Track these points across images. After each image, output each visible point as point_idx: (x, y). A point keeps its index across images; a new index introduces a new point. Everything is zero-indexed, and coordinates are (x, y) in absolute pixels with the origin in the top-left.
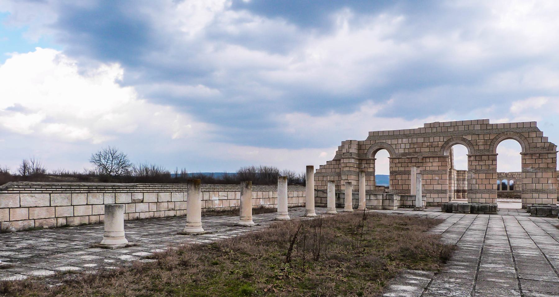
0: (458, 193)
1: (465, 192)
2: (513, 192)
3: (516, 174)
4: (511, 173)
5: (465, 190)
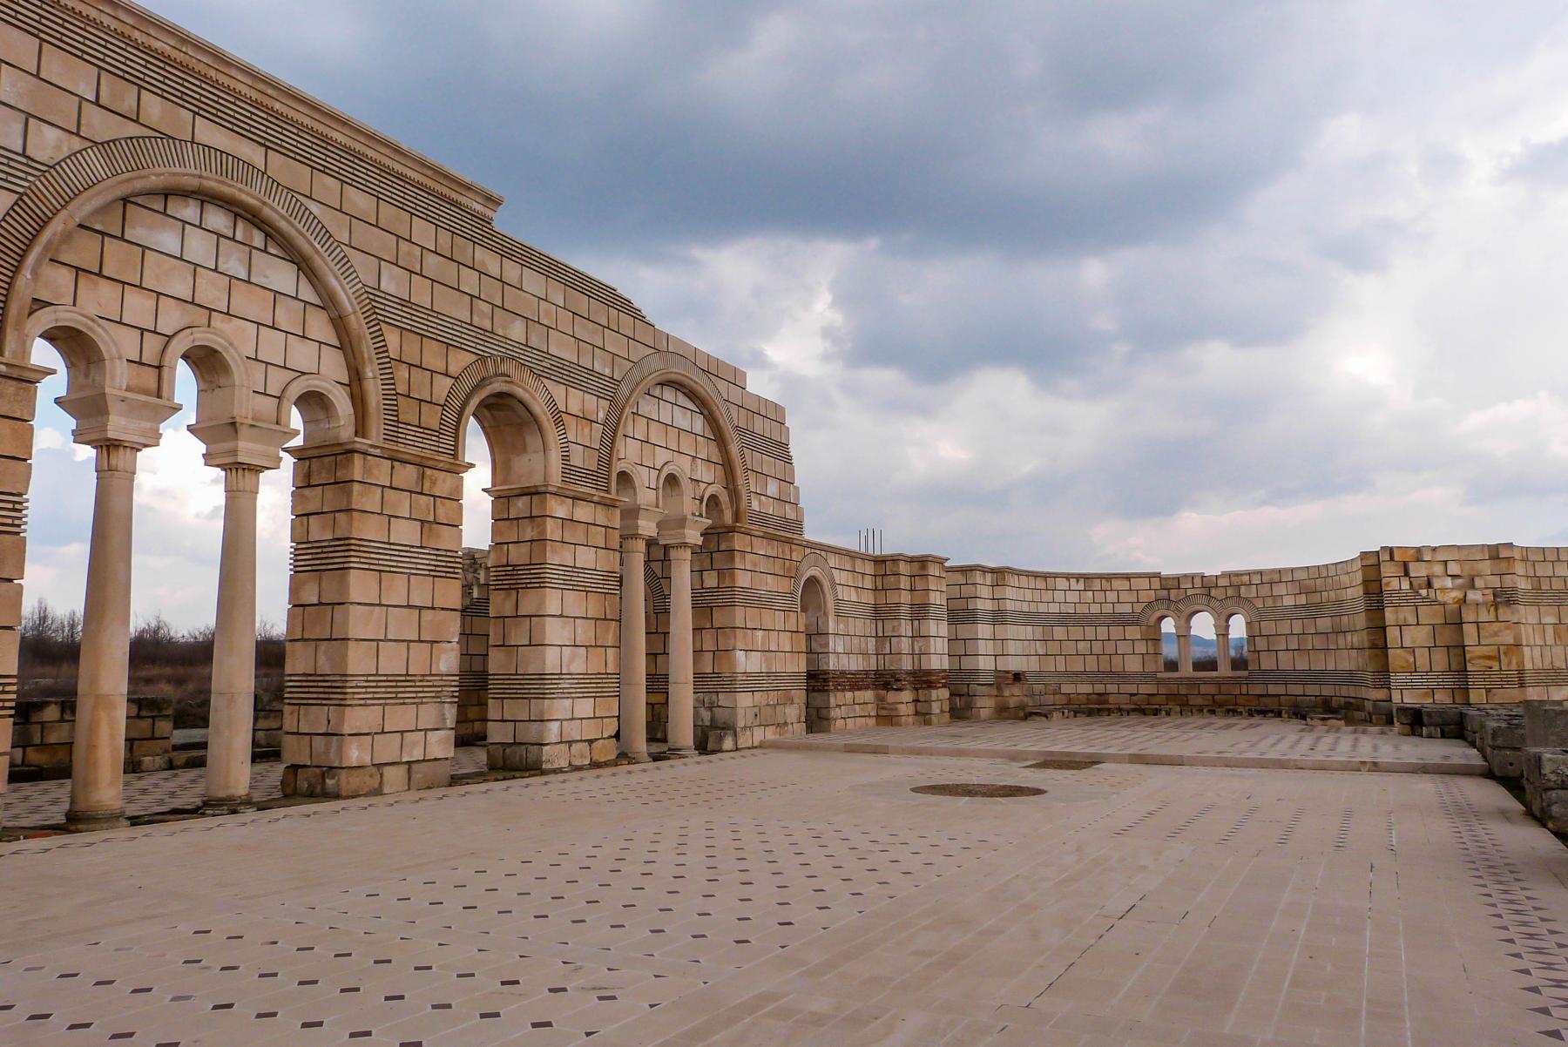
1: (930, 685)
2: (1248, 681)
3: (1256, 580)
4: (1229, 575)
5: (929, 672)
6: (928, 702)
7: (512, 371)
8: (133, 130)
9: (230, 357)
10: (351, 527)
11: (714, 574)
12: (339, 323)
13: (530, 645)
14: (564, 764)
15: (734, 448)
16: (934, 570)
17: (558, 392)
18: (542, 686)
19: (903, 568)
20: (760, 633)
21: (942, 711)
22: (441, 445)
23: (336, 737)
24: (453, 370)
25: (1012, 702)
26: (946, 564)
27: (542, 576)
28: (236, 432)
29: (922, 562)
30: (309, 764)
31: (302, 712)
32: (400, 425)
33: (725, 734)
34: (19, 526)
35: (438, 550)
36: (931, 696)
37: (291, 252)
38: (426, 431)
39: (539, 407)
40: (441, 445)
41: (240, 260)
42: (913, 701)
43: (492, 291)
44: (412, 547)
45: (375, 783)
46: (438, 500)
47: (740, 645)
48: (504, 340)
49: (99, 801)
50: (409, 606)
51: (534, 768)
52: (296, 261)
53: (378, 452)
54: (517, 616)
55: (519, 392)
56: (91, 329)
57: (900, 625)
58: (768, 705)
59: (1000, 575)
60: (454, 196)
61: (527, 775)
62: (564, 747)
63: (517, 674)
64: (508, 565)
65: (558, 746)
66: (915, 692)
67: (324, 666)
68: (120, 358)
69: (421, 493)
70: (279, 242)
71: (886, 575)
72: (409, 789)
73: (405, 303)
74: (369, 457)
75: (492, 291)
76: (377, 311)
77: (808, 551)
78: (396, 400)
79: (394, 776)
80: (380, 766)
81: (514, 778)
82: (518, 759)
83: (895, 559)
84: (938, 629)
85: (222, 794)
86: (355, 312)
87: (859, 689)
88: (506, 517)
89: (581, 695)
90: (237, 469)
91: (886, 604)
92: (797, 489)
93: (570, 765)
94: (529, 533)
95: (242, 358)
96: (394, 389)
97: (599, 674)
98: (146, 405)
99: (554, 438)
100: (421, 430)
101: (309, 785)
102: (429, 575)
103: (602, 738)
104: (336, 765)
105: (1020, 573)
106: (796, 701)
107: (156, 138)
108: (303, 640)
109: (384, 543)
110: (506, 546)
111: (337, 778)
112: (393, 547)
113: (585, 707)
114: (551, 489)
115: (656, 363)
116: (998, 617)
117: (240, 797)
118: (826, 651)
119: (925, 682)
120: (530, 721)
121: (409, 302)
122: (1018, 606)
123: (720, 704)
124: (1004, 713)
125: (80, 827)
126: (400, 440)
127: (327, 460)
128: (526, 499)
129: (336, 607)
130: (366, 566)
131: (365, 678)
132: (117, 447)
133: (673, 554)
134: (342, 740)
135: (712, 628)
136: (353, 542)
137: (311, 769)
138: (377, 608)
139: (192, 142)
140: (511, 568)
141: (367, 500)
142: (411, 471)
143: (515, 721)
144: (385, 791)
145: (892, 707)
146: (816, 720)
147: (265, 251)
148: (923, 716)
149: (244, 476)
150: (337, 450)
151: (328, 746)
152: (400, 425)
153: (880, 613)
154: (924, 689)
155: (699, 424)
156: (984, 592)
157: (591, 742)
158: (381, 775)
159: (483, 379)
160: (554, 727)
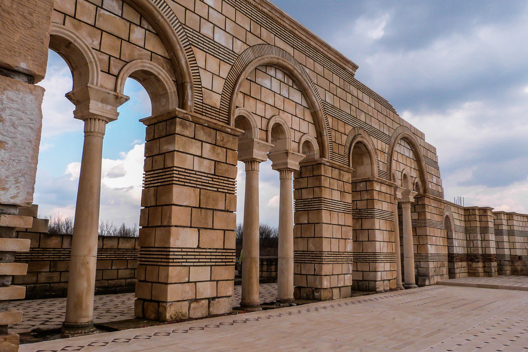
0: (470, 263)
1: (491, 260)
5: (490, 255)
6: (490, 267)
7: (362, 133)
8: (260, 42)
9: (285, 128)
10: (322, 193)
11: (416, 214)
12: (314, 115)
13: (368, 241)
14: (382, 289)
15: (423, 164)
16: (489, 213)
17: (375, 141)
18: (375, 258)
19: (477, 212)
20: (434, 238)
21: (495, 271)
22: (345, 161)
23: (318, 276)
24: (347, 132)
25: (519, 268)
26: (493, 211)
27: (373, 213)
28: (287, 156)
29: (485, 210)
30: (306, 286)
31: (302, 266)
32: (334, 154)
33: (426, 278)
34: (234, 191)
35: (345, 202)
36: (491, 265)
37: (300, 87)
38: (341, 156)
39: (370, 147)
40: (345, 161)
41: (286, 91)
42: (483, 267)
43: (355, 102)
44: (338, 201)
45: (330, 295)
46: (345, 183)
47: (429, 243)
48: (359, 121)
49: (254, 299)
50: (338, 225)
51: (372, 290)
52: (301, 91)
53: (328, 164)
54: (362, 229)
55: (365, 141)
56: (249, 116)
57: (477, 235)
58: (438, 267)
59: (510, 216)
60: (344, 66)
61: (372, 293)
62: (382, 282)
63: (363, 252)
64: (357, 209)
65: (381, 282)
66: (483, 263)
67: (312, 248)
68: (257, 127)
69: (340, 180)
70: (297, 84)
71: (470, 215)
72: (340, 298)
73: (333, 107)
74: (325, 166)
75: (355, 102)
76: (326, 109)
77: (446, 205)
78: (332, 144)
79: (336, 291)
80: (331, 288)
81: (369, 294)
82: (365, 286)
83: (474, 209)
84: (492, 237)
85: (286, 298)
86: (320, 110)
87: (462, 261)
88: (355, 190)
89: (386, 261)
90: (288, 170)
91: (470, 227)
92: (441, 180)
93: (384, 290)
94: (366, 196)
95: (288, 128)
96: (331, 140)
97: (391, 253)
98: (264, 145)
99: (375, 159)
100: (339, 156)
101: (307, 294)
102: (343, 213)
103: (393, 279)
104: (319, 287)
105: (518, 215)
106: (445, 266)
107: (265, 44)
108: (301, 237)
109: (330, 199)
110: (355, 202)
111: (320, 293)
112: (333, 201)
113: (387, 266)
114: (375, 179)
115: (400, 130)
116: (511, 233)
117: (292, 299)
118: (452, 245)
119: (488, 259)
120: (370, 271)
121: (334, 106)
122: (520, 229)
123: (421, 266)
124: (515, 272)
125: (254, 309)
126: (334, 159)
127: (309, 167)
128: (364, 183)
129: (316, 224)
130: (326, 209)
131: (327, 253)
132: (254, 161)
133: (403, 206)
134: (322, 278)
135: (416, 235)
136: (323, 199)
137: (307, 289)
138: (330, 225)
139: (275, 46)
140: (358, 210)
141: (325, 183)
142: (336, 172)
143: (363, 271)
144: (334, 298)
145: (475, 269)
146: (452, 274)
147: (293, 87)
148: (488, 274)
149: (288, 173)
150: (315, 163)
151: (315, 281)
152: (334, 154)
153: (468, 231)
154: (488, 262)
155: (411, 155)
156: (504, 222)
157: (389, 280)
158: (332, 292)
159: (355, 136)
160: (379, 273)
